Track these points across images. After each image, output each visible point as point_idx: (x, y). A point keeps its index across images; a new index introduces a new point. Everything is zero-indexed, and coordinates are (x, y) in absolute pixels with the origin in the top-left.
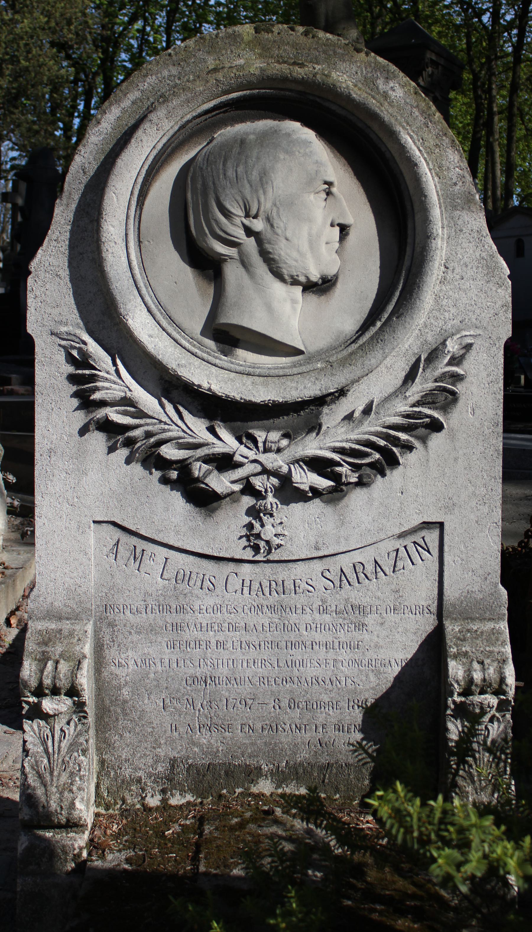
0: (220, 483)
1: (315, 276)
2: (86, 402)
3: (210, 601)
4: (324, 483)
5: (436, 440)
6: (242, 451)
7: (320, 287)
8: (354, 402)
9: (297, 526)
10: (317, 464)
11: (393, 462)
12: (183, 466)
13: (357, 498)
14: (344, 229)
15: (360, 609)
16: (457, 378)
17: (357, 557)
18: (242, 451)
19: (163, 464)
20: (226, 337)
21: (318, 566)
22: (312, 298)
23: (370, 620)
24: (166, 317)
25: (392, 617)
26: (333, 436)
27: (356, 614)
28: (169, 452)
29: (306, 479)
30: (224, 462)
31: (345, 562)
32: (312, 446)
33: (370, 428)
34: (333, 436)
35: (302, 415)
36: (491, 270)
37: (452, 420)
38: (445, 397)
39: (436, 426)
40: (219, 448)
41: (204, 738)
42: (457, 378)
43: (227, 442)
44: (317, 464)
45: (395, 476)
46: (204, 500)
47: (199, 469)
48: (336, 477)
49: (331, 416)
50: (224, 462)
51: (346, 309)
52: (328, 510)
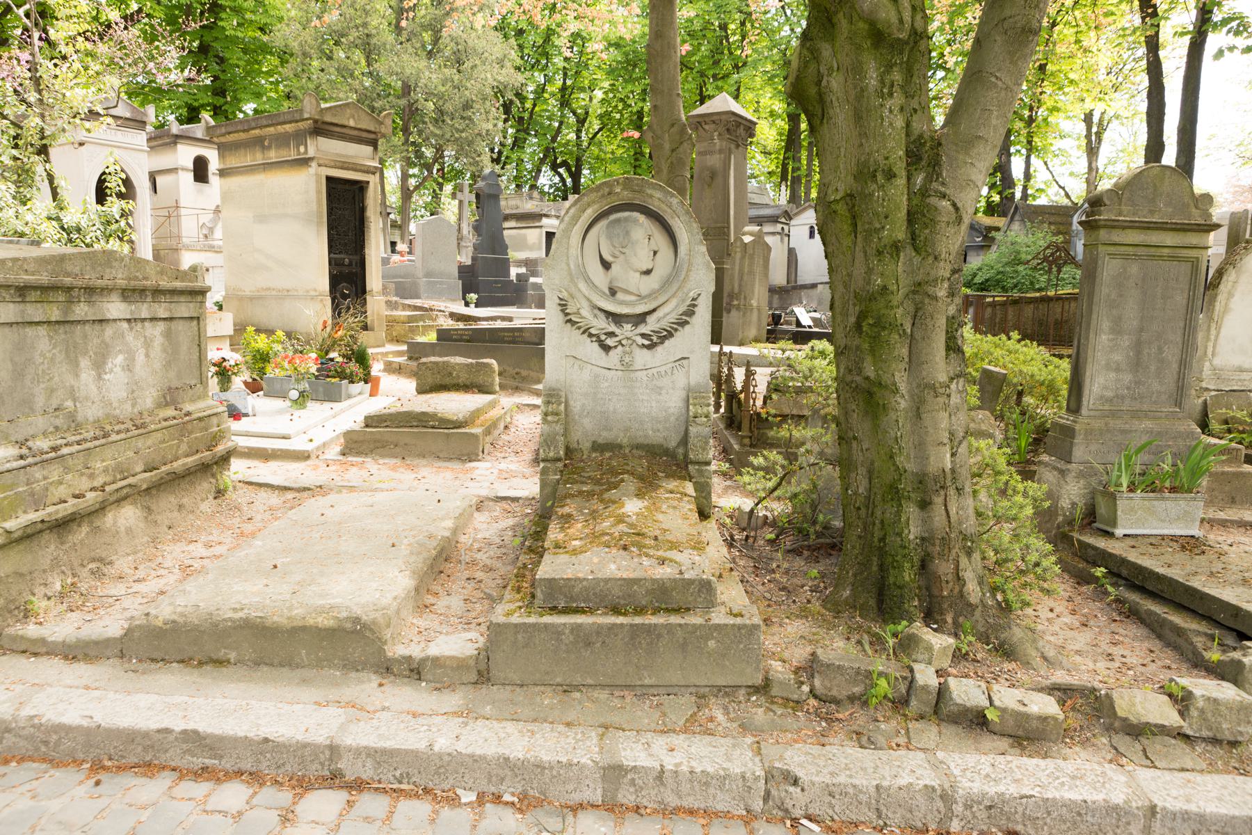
0: (610, 342)
1: (644, 269)
4: (647, 342)
5: (687, 327)
6: (617, 331)
10: (643, 335)
12: (598, 336)
13: (659, 349)
14: (655, 253)
15: (661, 388)
19: (591, 335)
22: (645, 278)
23: (664, 392)
25: (671, 391)
26: (651, 325)
27: (658, 390)
28: (593, 331)
29: (640, 341)
30: (612, 334)
31: (654, 371)
32: (643, 329)
33: (664, 324)
34: (651, 325)
35: (641, 318)
36: (708, 266)
38: (690, 312)
39: (687, 323)
40: (610, 330)
41: (604, 434)
42: (695, 306)
43: (612, 328)
44: (643, 335)
45: (672, 340)
46: (606, 348)
47: (603, 337)
49: (651, 319)
50: (612, 334)
51: (652, 283)
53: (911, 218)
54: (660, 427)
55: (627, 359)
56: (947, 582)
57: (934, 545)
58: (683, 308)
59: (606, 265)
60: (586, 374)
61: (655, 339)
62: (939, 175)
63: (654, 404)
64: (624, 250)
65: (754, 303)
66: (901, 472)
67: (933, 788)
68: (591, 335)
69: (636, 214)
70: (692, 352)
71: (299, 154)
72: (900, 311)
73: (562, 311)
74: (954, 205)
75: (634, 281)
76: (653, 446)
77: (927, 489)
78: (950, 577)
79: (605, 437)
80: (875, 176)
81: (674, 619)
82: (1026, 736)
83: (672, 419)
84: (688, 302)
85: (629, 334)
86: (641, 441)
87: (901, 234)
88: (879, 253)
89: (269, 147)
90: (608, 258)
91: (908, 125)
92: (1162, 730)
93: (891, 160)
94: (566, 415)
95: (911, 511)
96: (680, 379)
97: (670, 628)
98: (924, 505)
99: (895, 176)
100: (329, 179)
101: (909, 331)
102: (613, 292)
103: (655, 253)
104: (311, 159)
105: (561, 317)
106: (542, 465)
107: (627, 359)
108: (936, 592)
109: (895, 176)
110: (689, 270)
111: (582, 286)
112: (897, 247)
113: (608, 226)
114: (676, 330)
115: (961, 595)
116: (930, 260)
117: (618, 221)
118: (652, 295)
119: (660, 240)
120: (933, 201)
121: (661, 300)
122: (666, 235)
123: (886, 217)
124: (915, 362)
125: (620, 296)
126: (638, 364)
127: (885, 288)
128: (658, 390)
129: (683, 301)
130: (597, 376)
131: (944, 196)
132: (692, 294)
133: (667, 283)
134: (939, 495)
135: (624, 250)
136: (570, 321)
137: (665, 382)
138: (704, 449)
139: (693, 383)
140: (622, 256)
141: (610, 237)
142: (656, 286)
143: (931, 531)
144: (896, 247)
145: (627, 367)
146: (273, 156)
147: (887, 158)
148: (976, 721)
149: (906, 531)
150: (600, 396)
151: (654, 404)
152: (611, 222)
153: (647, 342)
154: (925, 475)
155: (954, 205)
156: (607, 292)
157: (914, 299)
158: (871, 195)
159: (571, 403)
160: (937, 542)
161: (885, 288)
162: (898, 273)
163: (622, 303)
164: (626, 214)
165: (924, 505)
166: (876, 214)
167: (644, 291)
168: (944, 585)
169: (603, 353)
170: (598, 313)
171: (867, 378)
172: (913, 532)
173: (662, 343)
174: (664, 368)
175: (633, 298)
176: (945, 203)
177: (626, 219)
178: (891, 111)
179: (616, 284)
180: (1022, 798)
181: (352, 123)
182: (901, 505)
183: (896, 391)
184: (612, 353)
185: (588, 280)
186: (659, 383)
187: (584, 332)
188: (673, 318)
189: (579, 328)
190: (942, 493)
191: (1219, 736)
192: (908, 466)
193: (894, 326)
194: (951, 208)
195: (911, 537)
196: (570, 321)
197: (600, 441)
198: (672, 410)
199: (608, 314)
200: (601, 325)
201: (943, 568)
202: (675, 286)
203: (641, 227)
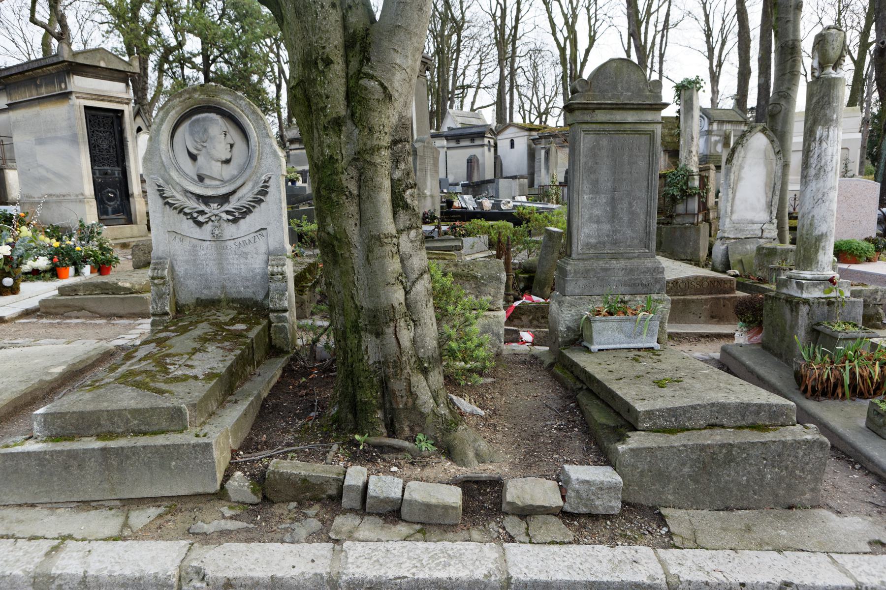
0: (201, 219)
1: (224, 158)
3: (203, 253)
4: (231, 218)
5: (263, 204)
7: (227, 162)
8: (239, 194)
9: (230, 230)
10: (228, 212)
11: (251, 212)
12: (191, 214)
13: (242, 221)
14: (232, 146)
15: (247, 254)
16: (267, 187)
17: (244, 239)
19: (186, 214)
20: (201, 178)
21: (233, 242)
22: (224, 166)
23: (249, 256)
25: (255, 256)
27: (245, 255)
29: (225, 216)
30: (202, 213)
31: (240, 240)
32: (227, 207)
33: (243, 202)
35: (224, 199)
37: (268, 198)
38: (264, 192)
39: (262, 201)
40: (201, 209)
41: (206, 292)
42: (267, 187)
44: (228, 212)
45: (252, 215)
46: (200, 224)
48: (234, 216)
50: (202, 213)
52: (234, 225)
53: (349, 96)
54: (249, 284)
55: (217, 232)
56: (402, 397)
57: (388, 367)
58: (257, 189)
59: (193, 157)
60: (187, 245)
61: (237, 214)
62: (369, 60)
63: (243, 267)
64: (205, 144)
65: (427, 192)
66: (358, 309)
67: (321, 575)
68: (186, 214)
69: (213, 115)
70: (269, 224)
71: (61, 89)
72: (344, 177)
73: (161, 195)
74: (382, 85)
75: (216, 169)
76: (245, 299)
77: (379, 320)
78: (404, 393)
79: (206, 294)
80: (316, 63)
81: (142, 441)
82: (430, 523)
83: (258, 277)
84: (261, 184)
85: (216, 212)
86: (234, 296)
87: (342, 110)
88: (325, 128)
89: (41, 86)
90: (194, 152)
91: (344, 18)
92: (546, 511)
93: (328, 50)
94: (173, 279)
95: (369, 341)
96: (262, 246)
97: (134, 450)
98: (379, 334)
99: (332, 62)
100: (86, 108)
101: (355, 192)
102: (201, 178)
103: (232, 146)
104: (71, 93)
105: (160, 202)
106: (152, 318)
107: (217, 232)
108: (395, 406)
109: (332, 62)
110: (260, 159)
111: (174, 174)
112: (338, 123)
113: (190, 126)
114: (254, 207)
115: (414, 406)
116: (366, 130)
117: (198, 120)
118: (233, 179)
119: (234, 135)
120: (364, 82)
121: (238, 183)
122: (239, 131)
123: (328, 97)
124: (363, 220)
125: (207, 181)
126: (227, 235)
127: (331, 157)
128: (245, 255)
129: (257, 183)
130: (194, 246)
131: (372, 77)
132: (263, 178)
133: (243, 169)
134: (389, 327)
135: (205, 144)
136: (167, 203)
137: (249, 248)
138: (281, 300)
139: (271, 248)
140: (204, 150)
141: (192, 134)
142: (235, 172)
143: (385, 356)
144: (337, 124)
145: (217, 239)
146: (44, 92)
147: (324, 48)
148: (393, 513)
149: (366, 358)
150: (199, 262)
151: (243, 267)
152: (192, 122)
153: (231, 218)
154: (377, 310)
155: (382, 85)
156: (196, 178)
157: (356, 167)
158: (315, 80)
159: (177, 268)
160: (391, 365)
161: (331, 157)
162: (344, 146)
163: (208, 187)
165: (379, 334)
166: (320, 96)
167: (226, 177)
168: (399, 399)
169: (198, 229)
170: (190, 195)
171: (328, 233)
172: (372, 356)
173: (244, 218)
174: (246, 238)
175: (218, 183)
176: (373, 84)
177: (204, 119)
178: (322, 7)
179: (204, 172)
180: (396, 578)
181: (102, 64)
182: (360, 337)
183: (349, 244)
184: (205, 227)
185: (179, 170)
186: (245, 250)
187: (180, 212)
188: (250, 196)
189: (175, 208)
190: (392, 324)
191: (594, 512)
192: (364, 304)
193: (342, 190)
194: (378, 87)
195: (371, 362)
196: (167, 203)
197: (203, 297)
198: (257, 271)
199: (199, 197)
200: (192, 205)
201: (397, 386)
202: (248, 172)
203: (217, 125)
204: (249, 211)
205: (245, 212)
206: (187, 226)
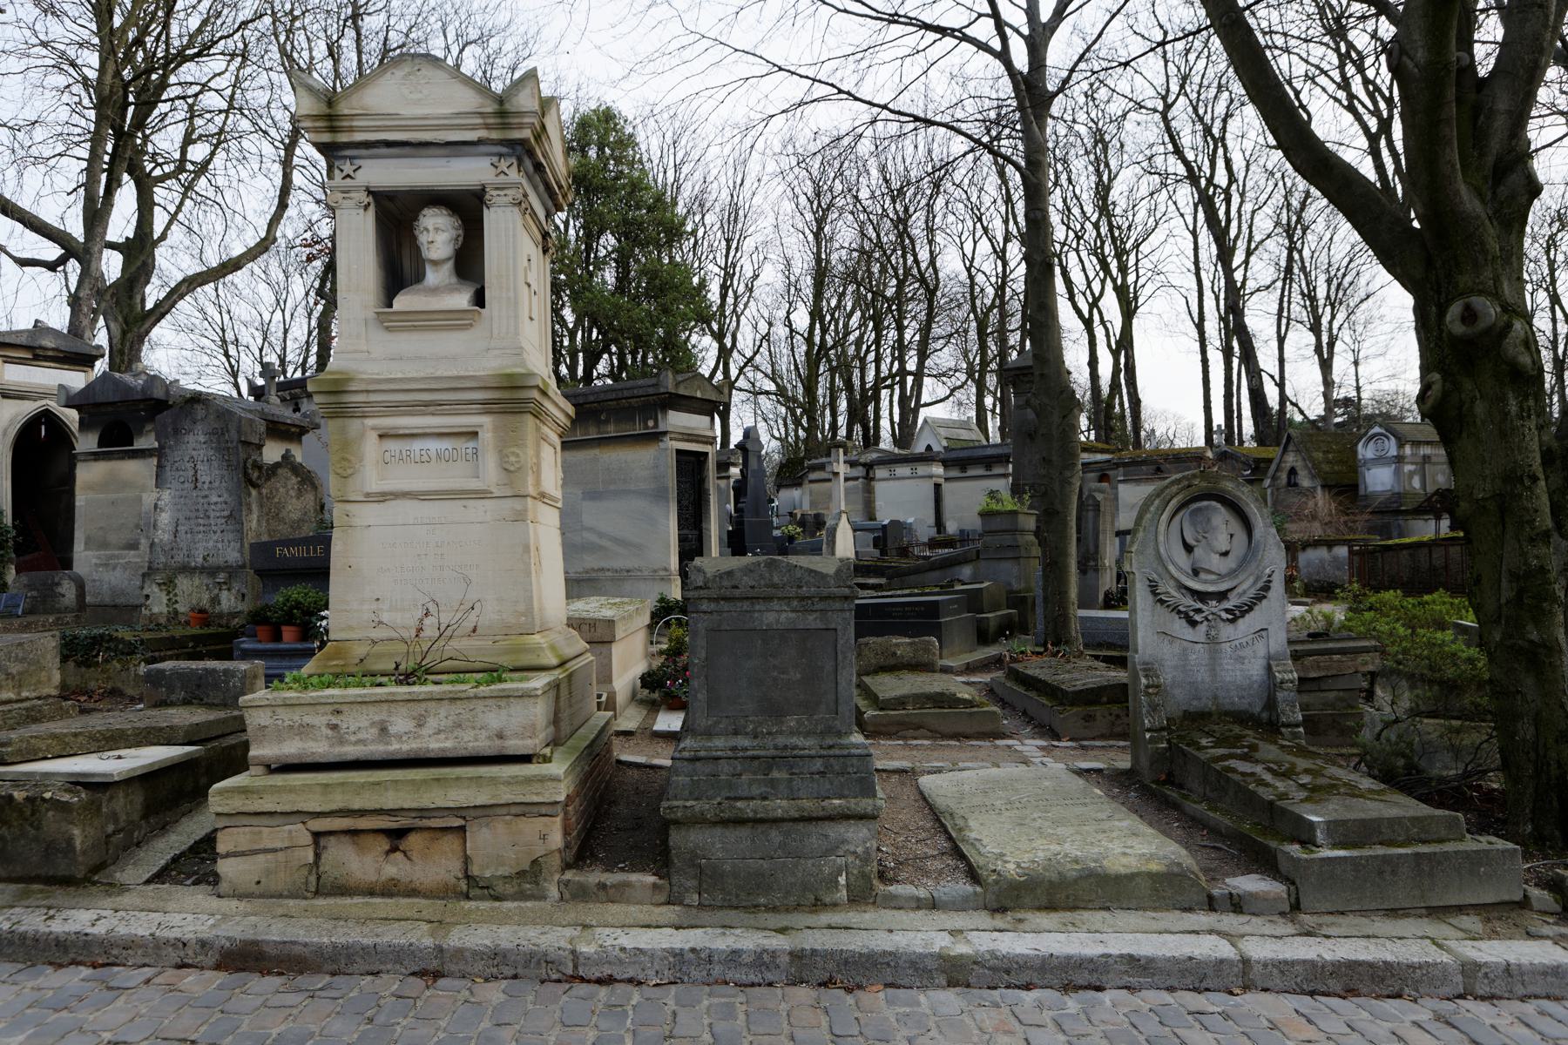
0: (1198, 618)
2: (1154, 593)
6: (1204, 608)
7: (1225, 554)
8: (1239, 590)
10: (1227, 611)
13: (1241, 621)
18: (1204, 608)
19: (1179, 612)
24: (1180, 569)
27: (1241, 660)
29: (1224, 615)
30: (1199, 611)
33: (1245, 599)
35: (1222, 596)
37: (1271, 594)
44: (1227, 611)
49: (1231, 595)
50: (1199, 611)
58: (1260, 584)
59: (1189, 549)
60: (1177, 648)
65: (1107, 563)
68: (1179, 612)
71: (647, 427)
72: (1557, 586)
75: (1216, 563)
79: (1196, 705)
86: (1228, 707)
87: (1549, 523)
89: (607, 422)
90: (1190, 541)
96: (1261, 649)
100: (679, 452)
102: (1196, 572)
104: (665, 433)
105: (1150, 598)
117: (1199, 509)
118: (1232, 573)
119: (1236, 526)
125: (1203, 576)
127: (1542, 567)
128: (1241, 660)
130: (1185, 650)
132: (1268, 571)
133: (1243, 563)
137: (1247, 652)
141: (1194, 524)
142: (1234, 566)
144: (1546, 535)
145: (1212, 641)
146: (611, 430)
163: (1205, 582)
164: (1205, 503)
166: (1527, 510)
167: (1224, 571)
171: (1532, 642)
177: (1207, 508)
181: (699, 395)
184: (1199, 627)
188: (1252, 593)
197: (1192, 709)
200: (1188, 602)
203: (1221, 518)
204: (1251, 609)
205: (1249, 608)
206: (1179, 627)
